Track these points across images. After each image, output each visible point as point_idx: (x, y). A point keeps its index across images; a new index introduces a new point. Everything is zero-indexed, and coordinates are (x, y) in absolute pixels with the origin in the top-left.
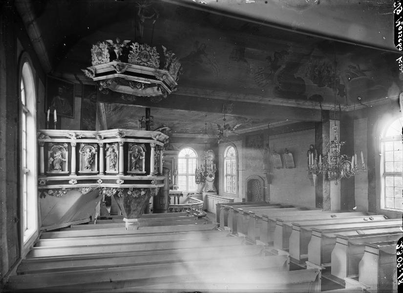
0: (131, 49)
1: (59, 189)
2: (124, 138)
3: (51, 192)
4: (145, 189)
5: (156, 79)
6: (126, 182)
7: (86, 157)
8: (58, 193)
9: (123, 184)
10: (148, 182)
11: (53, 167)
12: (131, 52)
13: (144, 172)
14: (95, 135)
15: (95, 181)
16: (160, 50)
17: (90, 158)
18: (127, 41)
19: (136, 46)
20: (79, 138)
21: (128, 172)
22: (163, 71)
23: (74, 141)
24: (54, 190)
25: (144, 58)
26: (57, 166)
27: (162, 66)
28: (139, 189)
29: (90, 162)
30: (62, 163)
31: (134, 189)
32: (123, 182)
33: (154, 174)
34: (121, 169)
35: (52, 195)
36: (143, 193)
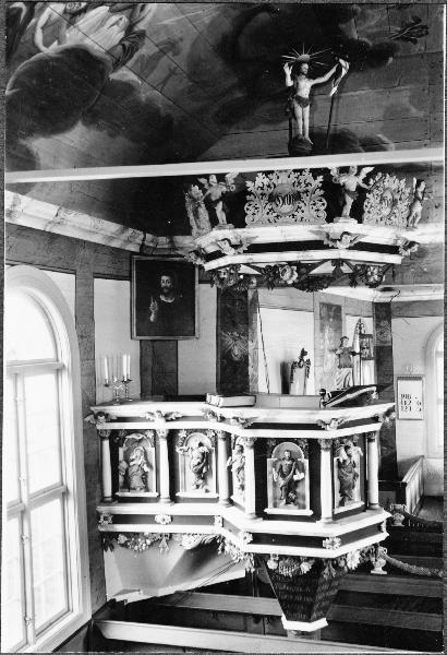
1: (136, 534)
2: (249, 428)
3: (122, 539)
4: (309, 559)
6: (258, 538)
7: (189, 460)
8: (135, 544)
9: (251, 542)
10: (316, 542)
11: (127, 485)
13: (308, 512)
14: (203, 410)
15: (209, 520)
17: (199, 464)
20: (172, 420)
21: (266, 510)
23: (163, 427)
24: (127, 534)
26: (136, 481)
28: (297, 559)
30: (144, 478)
31: (282, 557)
32: (250, 538)
34: (247, 498)
35: (125, 545)
36: (305, 567)
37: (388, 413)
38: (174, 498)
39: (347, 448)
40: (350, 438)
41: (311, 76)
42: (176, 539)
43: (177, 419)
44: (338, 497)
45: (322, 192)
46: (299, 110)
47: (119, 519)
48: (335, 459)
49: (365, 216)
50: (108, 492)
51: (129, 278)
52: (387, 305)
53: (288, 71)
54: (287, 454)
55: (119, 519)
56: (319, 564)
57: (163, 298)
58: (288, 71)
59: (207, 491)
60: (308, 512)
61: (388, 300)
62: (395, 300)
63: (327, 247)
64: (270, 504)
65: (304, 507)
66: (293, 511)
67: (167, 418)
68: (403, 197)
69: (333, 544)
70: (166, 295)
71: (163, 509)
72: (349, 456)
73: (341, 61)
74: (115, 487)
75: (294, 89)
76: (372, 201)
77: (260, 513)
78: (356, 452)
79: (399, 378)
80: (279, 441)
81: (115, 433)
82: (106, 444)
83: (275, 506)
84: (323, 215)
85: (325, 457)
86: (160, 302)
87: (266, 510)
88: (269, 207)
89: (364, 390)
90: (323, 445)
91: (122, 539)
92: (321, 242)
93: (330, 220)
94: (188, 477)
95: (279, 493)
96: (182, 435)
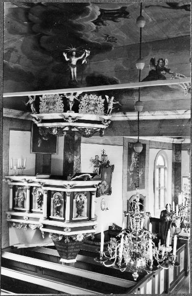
1: (18, 223)
5: (65, 121)
7: (36, 198)
8: (18, 226)
10: (62, 229)
11: (17, 206)
12: (40, 103)
22: (67, 114)
23: (27, 185)
24: (15, 223)
27: (66, 109)
28: (58, 235)
29: (38, 202)
33: (71, 221)
35: (14, 227)
36: (60, 238)
37: (100, 184)
38: (31, 211)
39: (80, 196)
40: (83, 192)
41: (77, 56)
43: (32, 182)
44: (75, 214)
45: (62, 101)
46: (72, 70)
47: (13, 217)
48: (74, 200)
49: (80, 111)
50: (11, 207)
51: (30, 131)
52: (180, 145)
53: (65, 55)
54: (57, 197)
55: (13, 217)
56: (64, 237)
57: (44, 138)
58: (65, 55)
59: (41, 210)
60: (63, 219)
61: (180, 143)
62: (183, 143)
65: (62, 217)
66: (58, 217)
67: (28, 182)
68: (100, 103)
69: (67, 230)
70: (45, 137)
72: (81, 199)
73: (86, 51)
75: (70, 61)
76: (82, 105)
77: (48, 218)
78: (85, 199)
79: (184, 177)
80: (55, 192)
81: (15, 186)
82: (11, 190)
83: (53, 215)
84: (63, 110)
85: (68, 199)
86: (43, 140)
87: (50, 217)
88: (46, 106)
89: (84, 175)
90: (67, 194)
91: (14, 224)
93: (65, 111)
94: (35, 204)
95: (55, 211)
96: (34, 188)
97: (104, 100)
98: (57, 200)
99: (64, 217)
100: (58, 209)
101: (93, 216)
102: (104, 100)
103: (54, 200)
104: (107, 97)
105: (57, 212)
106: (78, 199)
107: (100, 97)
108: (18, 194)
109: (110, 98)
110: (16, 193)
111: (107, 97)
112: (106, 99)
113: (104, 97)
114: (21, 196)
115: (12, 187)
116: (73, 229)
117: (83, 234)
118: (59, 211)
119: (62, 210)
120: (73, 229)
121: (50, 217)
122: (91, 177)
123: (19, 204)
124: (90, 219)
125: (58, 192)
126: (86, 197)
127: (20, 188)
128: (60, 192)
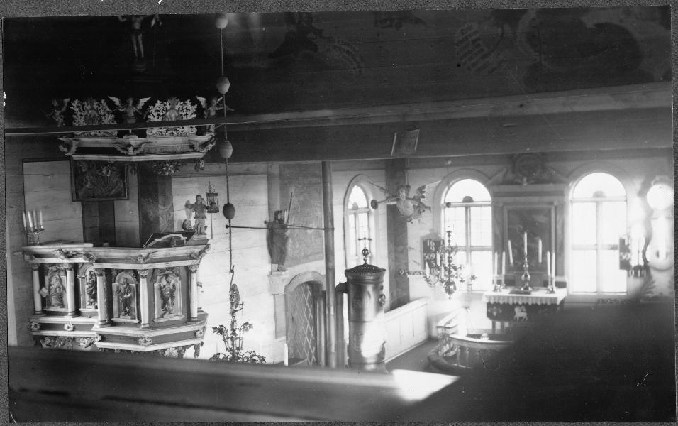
0: (73, 112)
7: (85, 287)
11: (50, 304)
16: (111, 105)
17: (90, 287)
18: (67, 101)
19: (78, 107)
25: (94, 125)
29: (90, 293)
38: (77, 313)
42: (77, 340)
44: (158, 310)
48: (156, 285)
50: (38, 307)
54: (122, 281)
63: (119, 154)
64: (116, 315)
65: (135, 318)
66: (128, 319)
71: (68, 319)
74: (45, 302)
80: (118, 271)
82: (36, 274)
87: (113, 319)
90: (141, 274)
92: (114, 149)
94: (85, 298)
95: (122, 306)
97: (195, 106)
98: (122, 288)
99: (139, 317)
100: (127, 303)
101: (195, 314)
102: (195, 106)
103: (118, 287)
104: (202, 100)
105: (125, 310)
106: (164, 283)
107: (188, 103)
108: (50, 281)
109: (209, 103)
110: (47, 278)
111: (202, 100)
112: (199, 103)
113: (194, 102)
114: (55, 283)
115: (36, 267)
116: (156, 340)
117: (176, 348)
118: (130, 307)
119: (134, 305)
120: (156, 340)
121: (113, 319)
122: (183, 238)
123: (54, 300)
124: (189, 319)
125: (123, 270)
126: (178, 278)
127: (53, 268)
128: (127, 271)
